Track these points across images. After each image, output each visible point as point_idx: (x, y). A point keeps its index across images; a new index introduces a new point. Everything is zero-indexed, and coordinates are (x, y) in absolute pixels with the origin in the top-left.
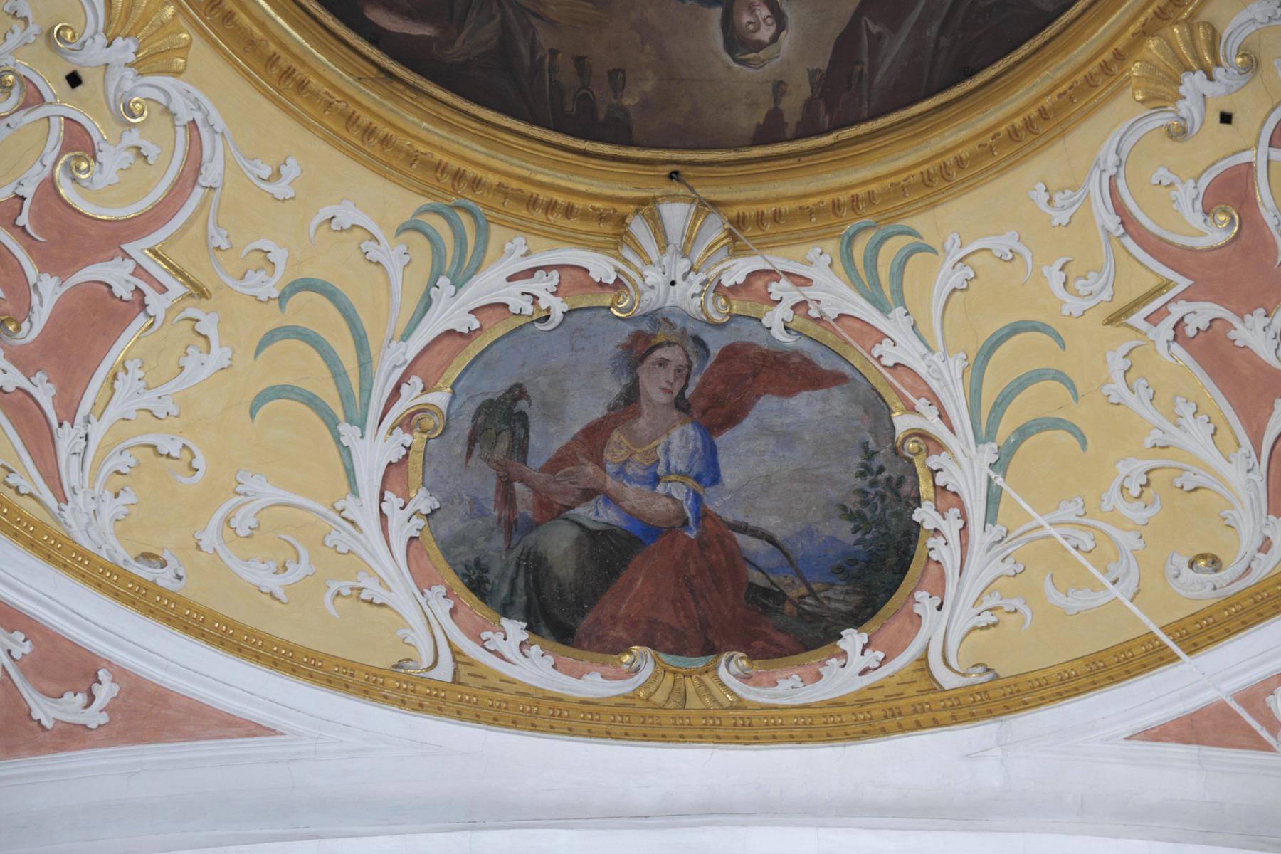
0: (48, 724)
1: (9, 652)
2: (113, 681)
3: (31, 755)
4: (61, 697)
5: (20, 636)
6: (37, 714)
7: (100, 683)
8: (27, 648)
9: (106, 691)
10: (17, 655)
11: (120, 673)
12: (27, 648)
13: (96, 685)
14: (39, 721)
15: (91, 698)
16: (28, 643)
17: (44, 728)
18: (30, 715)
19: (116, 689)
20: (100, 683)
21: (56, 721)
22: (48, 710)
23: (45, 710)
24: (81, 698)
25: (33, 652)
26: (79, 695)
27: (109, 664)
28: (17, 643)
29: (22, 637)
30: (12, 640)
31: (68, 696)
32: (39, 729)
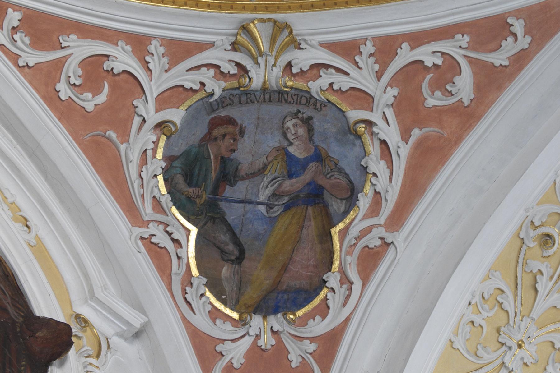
0: (506, 63)
1: (460, 47)
2: (518, 19)
3: (510, 83)
4: (501, 46)
5: (459, 36)
6: (497, 63)
7: (512, 25)
8: (467, 38)
9: (518, 26)
10: (465, 45)
11: (517, 13)
12: (467, 38)
13: (512, 27)
14: (501, 65)
15: (515, 35)
16: (465, 36)
17: (506, 66)
18: (495, 66)
19: (522, 21)
20: (512, 25)
21: (509, 58)
22: (501, 57)
23: (499, 59)
24: (510, 39)
25: (471, 38)
26: (508, 39)
27: (510, 13)
28: (460, 40)
29: (460, 36)
30: (457, 41)
31: (504, 43)
32: (504, 68)
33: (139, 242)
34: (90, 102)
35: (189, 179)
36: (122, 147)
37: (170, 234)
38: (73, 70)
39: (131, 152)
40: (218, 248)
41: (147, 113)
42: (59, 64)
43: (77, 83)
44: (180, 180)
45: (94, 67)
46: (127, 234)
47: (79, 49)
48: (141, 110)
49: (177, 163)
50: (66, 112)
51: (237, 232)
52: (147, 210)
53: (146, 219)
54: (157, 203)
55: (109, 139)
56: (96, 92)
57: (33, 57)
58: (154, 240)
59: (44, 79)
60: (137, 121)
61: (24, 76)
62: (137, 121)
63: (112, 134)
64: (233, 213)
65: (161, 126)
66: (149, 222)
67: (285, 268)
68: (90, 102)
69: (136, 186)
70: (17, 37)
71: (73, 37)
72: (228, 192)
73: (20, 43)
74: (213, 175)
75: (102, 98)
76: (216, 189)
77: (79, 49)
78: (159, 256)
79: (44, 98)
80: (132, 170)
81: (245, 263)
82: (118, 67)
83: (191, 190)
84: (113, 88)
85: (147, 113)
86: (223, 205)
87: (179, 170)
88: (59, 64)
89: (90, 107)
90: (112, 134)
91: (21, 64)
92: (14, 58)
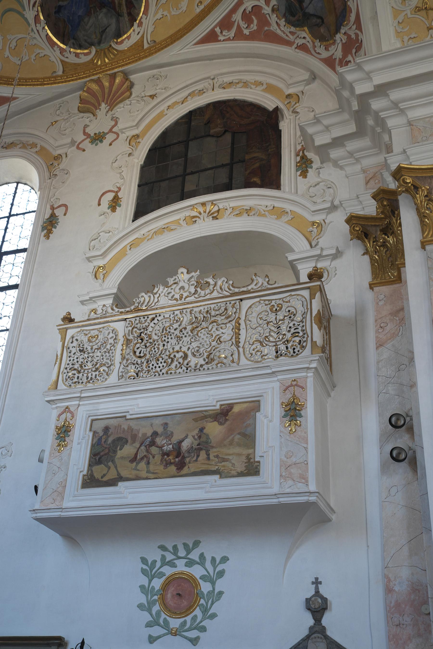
33: (296, 50)
34: (254, 27)
35: (293, 15)
36: (271, 28)
37: (301, 38)
38: (243, 25)
39: (274, 27)
40: (316, 25)
41: (267, 11)
42: (238, 26)
43: (247, 26)
44: (291, 18)
45: (246, 17)
46: (291, 51)
47: (237, 17)
48: (266, 12)
49: (287, 14)
50: (252, 37)
51: (316, 14)
52: (292, 38)
53: (293, 41)
54: (292, 33)
55: (267, 30)
56: (252, 22)
57: (232, 34)
58: (299, 45)
59: (240, 36)
60: (267, 16)
61: (236, 40)
62: (267, 16)
63: (266, 28)
64: (310, 10)
65: (273, 10)
66: (294, 41)
67: (335, 9)
68: (254, 27)
69: (283, 34)
70: (224, 33)
71: (234, 15)
72: (305, 5)
73: (226, 34)
74: (297, 5)
75: (255, 22)
76: (302, 8)
77: (237, 17)
78: (303, 48)
79: (245, 40)
80: (279, 32)
81: (325, 20)
82: (250, 9)
83: (296, 17)
84: (255, 15)
85: (267, 11)
86: (307, 11)
87: (289, 16)
88: (238, 26)
89: (255, 28)
90: (266, 28)
91: (232, 38)
92: (229, 39)
